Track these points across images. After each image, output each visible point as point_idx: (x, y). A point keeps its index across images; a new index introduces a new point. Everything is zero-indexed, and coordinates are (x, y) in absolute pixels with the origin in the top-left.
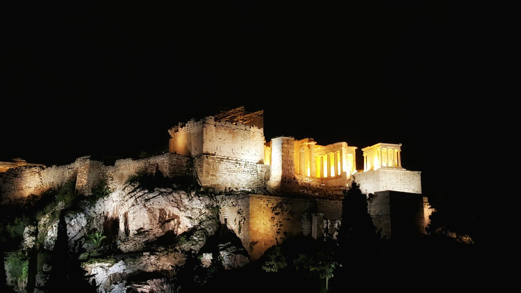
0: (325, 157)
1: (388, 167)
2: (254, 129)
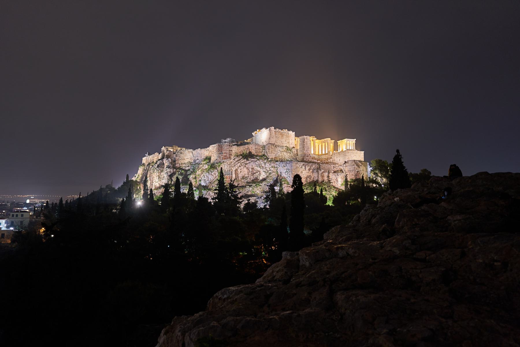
0: (324, 144)
1: (350, 150)
2: (291, 132)
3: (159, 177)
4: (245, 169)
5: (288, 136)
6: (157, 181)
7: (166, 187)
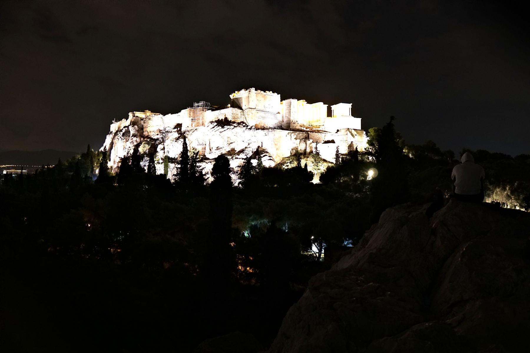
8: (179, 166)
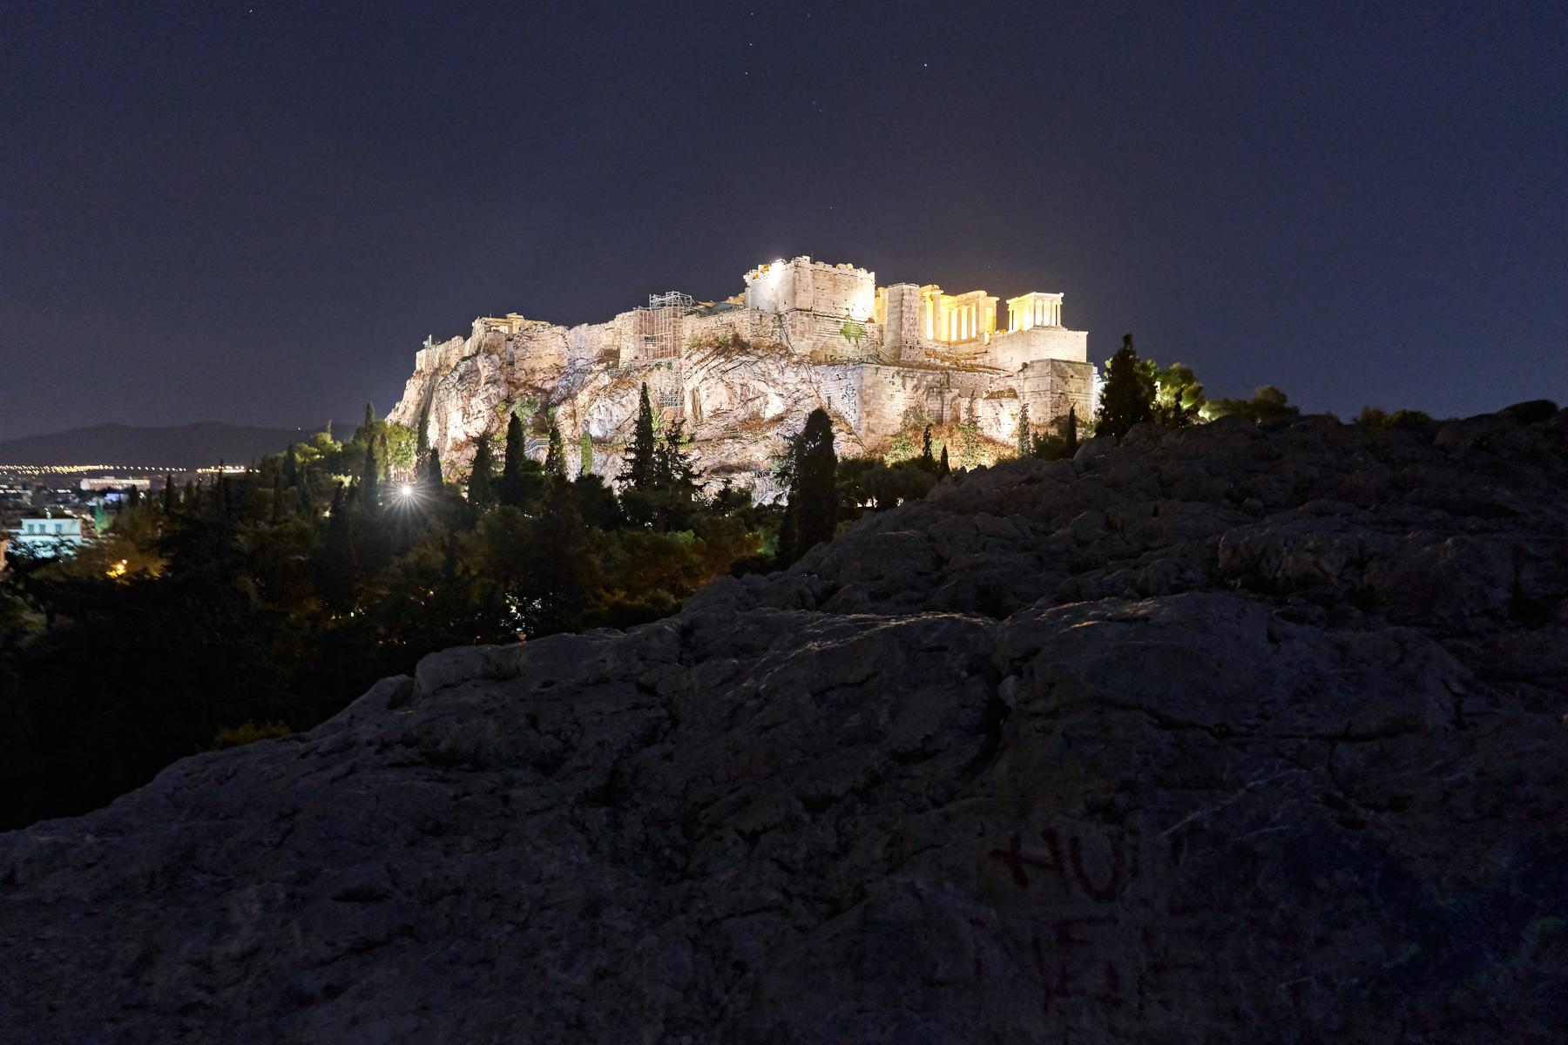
0: (964, 310)
2: (862, 273)
3: (466, 414)
4: (721, 388)
5: (851, 286)
6: (459, 424)
7: (482, 441)
8: (632, 456)
